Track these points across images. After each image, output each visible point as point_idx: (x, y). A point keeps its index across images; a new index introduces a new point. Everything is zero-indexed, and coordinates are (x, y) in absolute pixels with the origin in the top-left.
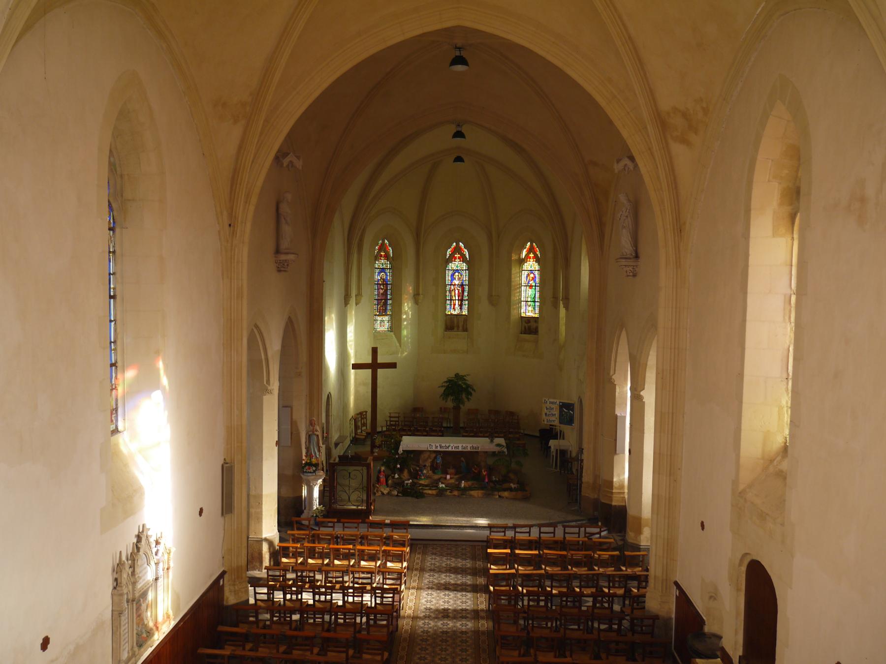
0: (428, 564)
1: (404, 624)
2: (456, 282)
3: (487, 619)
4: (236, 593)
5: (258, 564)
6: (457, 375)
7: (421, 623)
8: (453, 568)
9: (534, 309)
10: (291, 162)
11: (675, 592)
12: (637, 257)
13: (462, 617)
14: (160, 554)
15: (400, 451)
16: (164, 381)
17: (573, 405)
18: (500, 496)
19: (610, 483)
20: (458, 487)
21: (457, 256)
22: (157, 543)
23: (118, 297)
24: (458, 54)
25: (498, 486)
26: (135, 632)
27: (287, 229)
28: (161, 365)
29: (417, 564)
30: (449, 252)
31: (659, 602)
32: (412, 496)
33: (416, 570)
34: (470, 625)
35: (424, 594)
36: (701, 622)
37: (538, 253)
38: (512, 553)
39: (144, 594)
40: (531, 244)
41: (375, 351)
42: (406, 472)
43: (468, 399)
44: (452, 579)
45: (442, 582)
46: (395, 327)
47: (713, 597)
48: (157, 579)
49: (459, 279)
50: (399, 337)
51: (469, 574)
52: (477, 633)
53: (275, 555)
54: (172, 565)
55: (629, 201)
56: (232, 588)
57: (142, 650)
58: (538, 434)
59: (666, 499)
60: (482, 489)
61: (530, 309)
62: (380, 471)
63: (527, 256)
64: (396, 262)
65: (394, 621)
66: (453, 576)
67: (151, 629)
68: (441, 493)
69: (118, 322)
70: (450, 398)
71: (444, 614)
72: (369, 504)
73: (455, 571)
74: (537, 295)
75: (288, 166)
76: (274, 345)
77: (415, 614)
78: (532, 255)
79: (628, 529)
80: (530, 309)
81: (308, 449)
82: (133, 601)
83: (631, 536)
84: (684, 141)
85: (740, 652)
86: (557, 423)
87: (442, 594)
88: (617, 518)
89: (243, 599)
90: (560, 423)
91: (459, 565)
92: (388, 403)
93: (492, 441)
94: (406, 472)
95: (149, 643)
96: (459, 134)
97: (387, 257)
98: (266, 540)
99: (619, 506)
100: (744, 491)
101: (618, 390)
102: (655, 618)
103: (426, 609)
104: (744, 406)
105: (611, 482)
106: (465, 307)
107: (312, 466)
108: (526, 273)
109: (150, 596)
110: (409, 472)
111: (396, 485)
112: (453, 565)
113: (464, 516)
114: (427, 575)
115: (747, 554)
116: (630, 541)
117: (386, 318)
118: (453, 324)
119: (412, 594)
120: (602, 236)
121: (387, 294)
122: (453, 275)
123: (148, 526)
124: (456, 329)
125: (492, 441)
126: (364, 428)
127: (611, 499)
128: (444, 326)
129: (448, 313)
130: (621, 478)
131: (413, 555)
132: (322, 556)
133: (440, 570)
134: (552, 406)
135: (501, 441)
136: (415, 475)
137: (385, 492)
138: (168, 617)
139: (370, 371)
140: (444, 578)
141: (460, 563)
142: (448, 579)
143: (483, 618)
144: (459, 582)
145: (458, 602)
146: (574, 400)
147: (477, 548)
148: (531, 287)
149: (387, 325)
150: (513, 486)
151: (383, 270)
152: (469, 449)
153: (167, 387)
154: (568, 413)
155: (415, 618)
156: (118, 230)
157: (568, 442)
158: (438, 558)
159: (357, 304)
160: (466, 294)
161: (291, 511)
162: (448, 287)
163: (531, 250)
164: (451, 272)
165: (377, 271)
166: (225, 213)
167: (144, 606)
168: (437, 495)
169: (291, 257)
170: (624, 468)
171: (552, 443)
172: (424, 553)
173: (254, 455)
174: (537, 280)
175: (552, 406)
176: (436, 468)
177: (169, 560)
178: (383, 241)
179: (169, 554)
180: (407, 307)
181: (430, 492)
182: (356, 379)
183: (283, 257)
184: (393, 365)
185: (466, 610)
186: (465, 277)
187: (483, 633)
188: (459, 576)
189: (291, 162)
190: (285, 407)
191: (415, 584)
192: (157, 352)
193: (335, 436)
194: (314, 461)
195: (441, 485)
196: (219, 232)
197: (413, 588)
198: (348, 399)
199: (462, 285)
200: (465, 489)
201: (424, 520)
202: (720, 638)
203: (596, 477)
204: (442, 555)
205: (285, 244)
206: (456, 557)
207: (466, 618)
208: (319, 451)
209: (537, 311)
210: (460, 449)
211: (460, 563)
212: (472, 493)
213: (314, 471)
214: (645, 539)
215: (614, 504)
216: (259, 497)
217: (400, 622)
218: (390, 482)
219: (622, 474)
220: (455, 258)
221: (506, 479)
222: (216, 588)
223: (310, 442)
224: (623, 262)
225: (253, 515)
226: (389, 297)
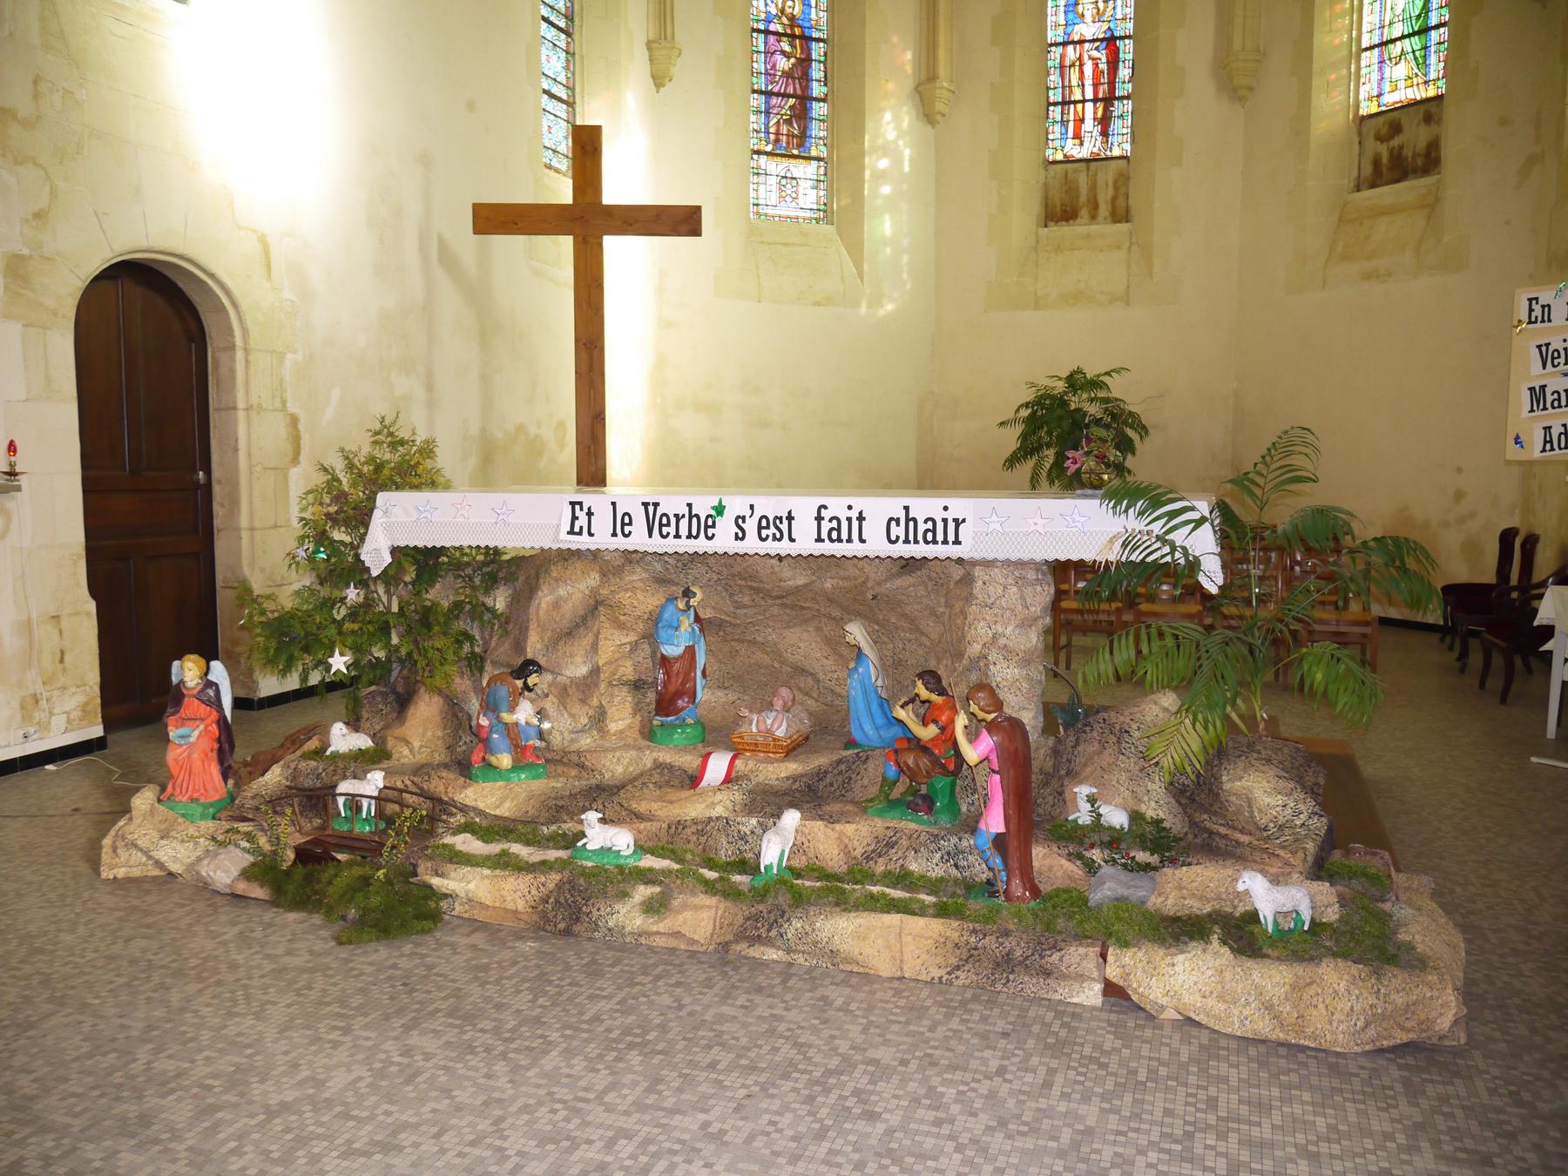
2: (1089, 29)
9: (1423, 63)
18: (1113, 991)
25: (1110, 886)
49: (1099, 16)
58: (1434, 616)
61: (1401, 71)
117: (806, 171)
118: (1068, 201)
121: (805, 78)
124: (1084, 213)
128: (1035, 208)
149: (809, 197)
159: (659, 80)
160: (1124, 72)
180: (891, 131)
199: (1110, 42)
209: (1436, 66)
210: (805, 542)
226: (817, 90)
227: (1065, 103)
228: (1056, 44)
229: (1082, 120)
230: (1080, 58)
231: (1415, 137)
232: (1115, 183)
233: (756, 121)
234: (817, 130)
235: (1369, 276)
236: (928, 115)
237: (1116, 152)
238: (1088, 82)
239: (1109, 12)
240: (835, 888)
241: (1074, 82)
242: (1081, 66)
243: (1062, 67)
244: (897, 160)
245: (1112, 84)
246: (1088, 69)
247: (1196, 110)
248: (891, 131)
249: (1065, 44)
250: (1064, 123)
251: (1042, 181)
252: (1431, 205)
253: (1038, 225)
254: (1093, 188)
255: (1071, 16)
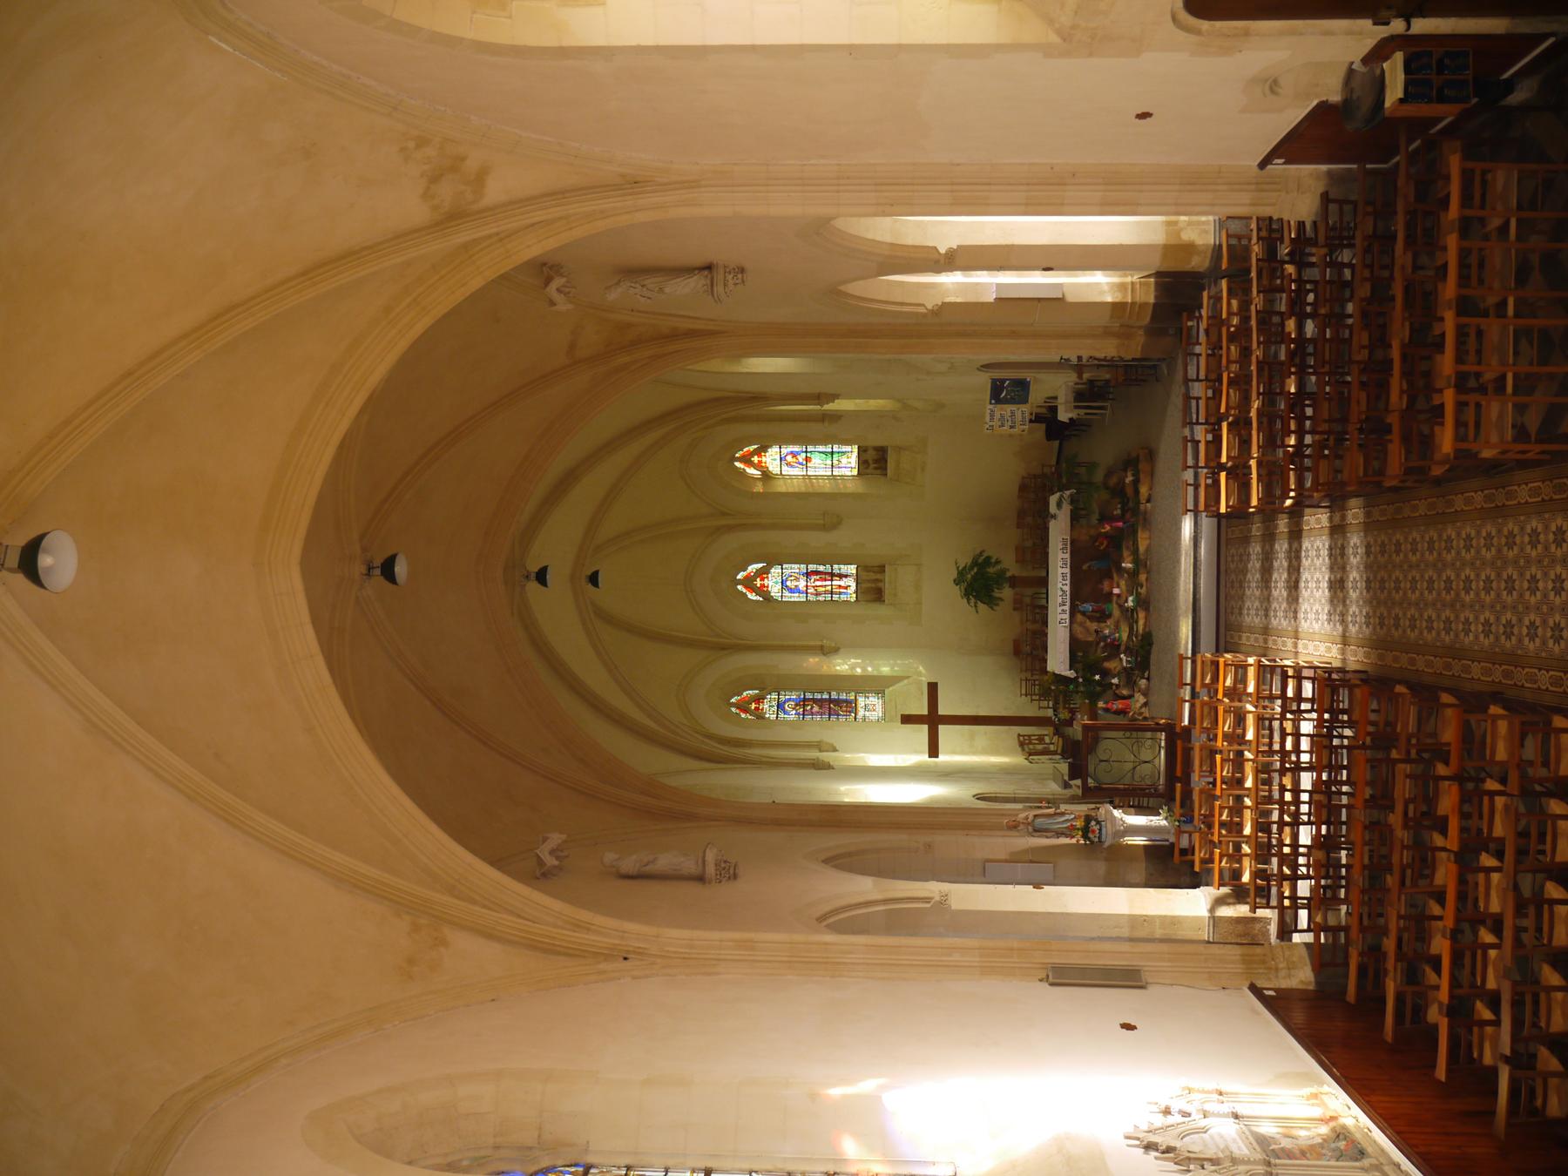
0: (1257, 620)
1: (1356, 659)
2: (802, 584)
3: (1343, 509)
4: (1291, 967)
5: (1258, 926)
6: (957, 582)
7: (1353, 629)
8: (1262, 576)
10: (552, 852)
11: (1278, 166)
12: (709, 267)
13: (1343, 554)
14: (1187, 1108)
15: (1071, 674)
16: (867, 1086)
17: (994, 381)
18: (1148, 501)
19: (1117, 307)
20: (1133, 574)
21: (758, 583)
22: (1167, 1112)
23: (710, 1164)
24: (378, 572)
25: (1131, 504)
26: (1333, 1163)
27: (665, 862)
28: (836, 1092)
29: (1256, 640)
30: (752, 596)
31: (1299, 195)
32: (1149, 653)
33: (1266, 641)
34: (1355, 539)
35: (1304, 626)
36: (1323, 110)
37: (752, 448)
38: (1231, 474)
39: (1263, 1141)
40: (739, 460)
41: (907, 719)
42: (1106, 665)
43: (998, 562)
44: (1280, 577)
45: (1285, 594)
46: (877, 685)
47: (1274, 86)
48: (1236, 1116)
49: (797, 579)
50: (893, 680)
51: (1272, 546)
52: (1368, 527)
53: (1240, 895)
54: (1212, 1085)
55: (618, 283)
56: (1282, 973)
57: (1370, 1150)
58: (1057, 443)
59: (1114, 192)
60: (1135, 532)
62: (1106, 710)
63: (758, 466)
64: (765, 686)
65: (1348, 676)
66: (1275, 576)
67: (1333, 1130)
68: (1143, 603)
69: (755, 1167)
70: (996, 594)
71: (1337, 587)
72: (1158, 728)
73: (1267, 571)
74: (821, 448)
75: (557, 858)
76: (864, 887)
77: (1339, 640)
78: (756, 459)
79: (1188, 268)
80: (844, 460)
81: (1059, 834)
82: (1269, 1164)
83: (1199, 263)
84: (479, 179)
85: (1366, 24)
86: (1025, 408)
87: (1305, 593)
88: (1177, 289)
89: (1304, 952)
90: (1025, 401)
91: (1258, 565)
92: (1007, 697)
93: (1054, 516)
94: (1106, 665)
95: (1358, 1136)
96: (541, 577)
97: (759, 699)
98: (1212, 910)
99: (1156, 290)
100: (1059, 32)
101: (948, 300)
102: (1326, 198)
103: (1329, 621)
104: (904, 41)
105: (1114, 305)
106: (845, 569)
107: (1088, 827)
108: (785, 468)
109: (1268, 1129)
110: (1107, 659)
111: (1131, 683)
112: (1258, 576)
113: (1178, 561)
114: (1274, 622)
115: (1174, 18)
116: (1207, 264)
117: (861, 701)
118: (872, 591)
119: (1306, 647)
120: (692, 334)
121: (822, 700)
123: (1130, 1130)
125: (1054, 516)
126: (1047, 739)
127: (1143, 305)
129: (853, 598)
130: (1106, 288)
131: (1243, 649)
132: (1238, 809)
133: (1267, 599)
134: (997, 415)
135: (1053, 499)
136: (1114, 649)
137: (1142, 700)
138: (1315, 1096)
139: (942, 728)
140: (1279, 591)
141: (1255, 564)
142: (1281, 584)
143: (1343, 517)
144: (1285, 564)
145: (1318, 563)
146: (984, 380)
147: (1231, 531)
148: (807, 459)
149: (873, 700)
150: (1129, 479)
151: (780, 706)
152: (1067, 556)
153: (882, 1081)
154: (1008, 390)
155: (1345, 641)
156: (590, 1159)
157: (1056, 388)
158: (1248, 604)
159: (835, 750)
160: (821, 568)
161: (1169, 866)
162: (811, 598)
163: (747, 460)
164: (786, 593)
165: (782, 715)
166: (602, 966)
167: (1286, 1143)
168: (1147, 610)
169: (711, 856)
170: (1088, 285)
171: (1064, 416)
172: (1239, 628)
173: (1056, 927)
174: (796, 449)
175: (997, 415)
176: (1103, 612)
177: (1204, 1092)
178: (733, 705)
179: (1190, 1091)
180: (843, 665)
181: (1141, 622)
182: (962, 753)
183: (711, 870)
184: (933, 688)
185: (1331, 548)
186: (794, 569)
187: (1368, 514)
188: (1276, 564)
189: (552, 852)
190: (984, 872)
191: (1290, 642)
192: (813, 1097)
193: (1054, 788)
194: (1079, 824)
195: (1130, 603)
196: (634, 978)
197: (1295, 645)
198: (994, 765)
199: (808, 574)
200: (1136, 561)
201: (1185, 630)
202: (1351, 72)
203: (1107, 333)
204: (1242, 598)
205: (689, 866)
206: (1244, 571)
207: (1343, 548)
208: (1063, 814)
209: (848, 448)
210: (1067, 570)
211: (1255, 564)
212: (1142, 549)
213: (1098, 822)
214: (1200, 230)
215: (1152, 300)
216: (1135, 921)
217: (1352, 666)
218: (1125, 692)
219: (1099, 285)
221: (1119, 492)
222: (1278, 1004)
223: (1046, 830)
224: (719, 289)
225: (1167, 938)
226: (826, 696)
231: (871, 455)
233: (842, 719)
234: (843, 696)
235: (923, 470)
236: (835, 651)
240: (1135, 552)
244: (856, 665)
247: (842, 538)
248: (843, 665)
252: (899, 449)
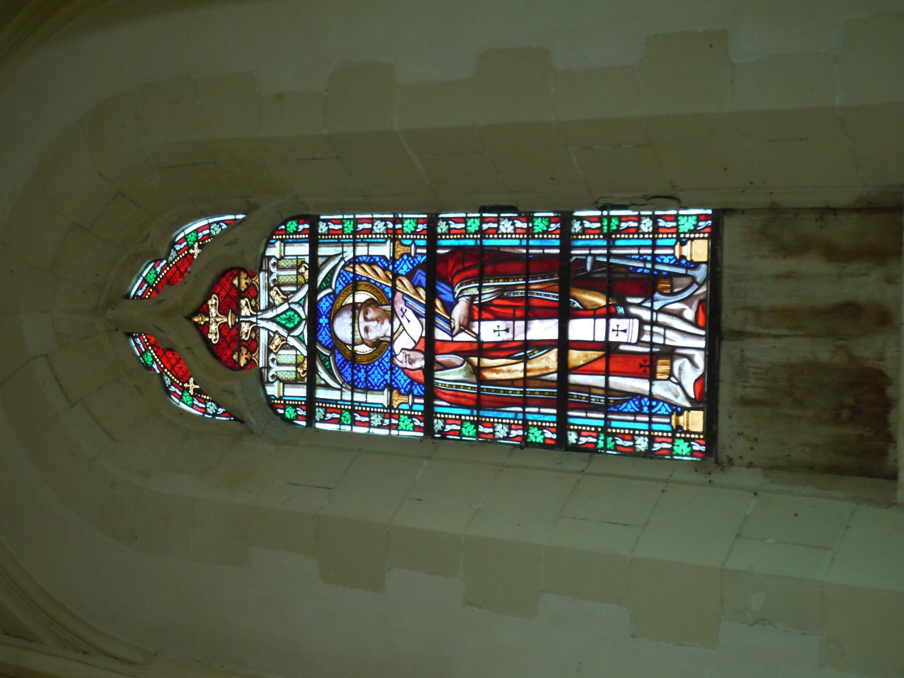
49: (384, 303)
122: (352, 366)
124: (866, 350)
128: (826, 508)
160: (507, 232)
186: (376, 244)
199: (438, 272)
220: (230, 334)
227: (563, 396)
228: (429, 415)
229: (608, 348)
230: (464, 352)
232: (785, 250)
237: (699, 250)
238: (518, 331)
239: (379, 276)
241: (517, 370)
242: (482, 349)
243: (479, 403)
245: (529, 265)
246: (490, 331)
249: (430, 392)
250: (612, 401)
251: (755, 479)
253: (890, 503)
254: (793, 319)
255: (376, 377)
